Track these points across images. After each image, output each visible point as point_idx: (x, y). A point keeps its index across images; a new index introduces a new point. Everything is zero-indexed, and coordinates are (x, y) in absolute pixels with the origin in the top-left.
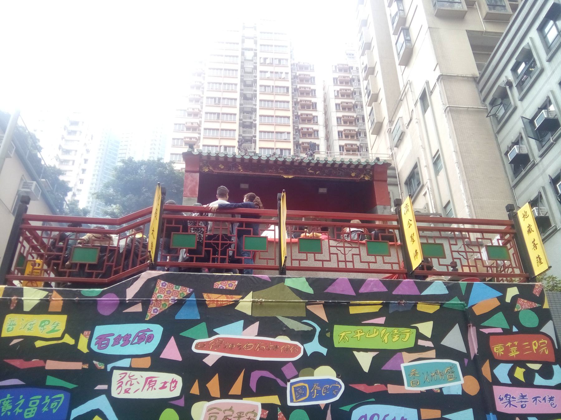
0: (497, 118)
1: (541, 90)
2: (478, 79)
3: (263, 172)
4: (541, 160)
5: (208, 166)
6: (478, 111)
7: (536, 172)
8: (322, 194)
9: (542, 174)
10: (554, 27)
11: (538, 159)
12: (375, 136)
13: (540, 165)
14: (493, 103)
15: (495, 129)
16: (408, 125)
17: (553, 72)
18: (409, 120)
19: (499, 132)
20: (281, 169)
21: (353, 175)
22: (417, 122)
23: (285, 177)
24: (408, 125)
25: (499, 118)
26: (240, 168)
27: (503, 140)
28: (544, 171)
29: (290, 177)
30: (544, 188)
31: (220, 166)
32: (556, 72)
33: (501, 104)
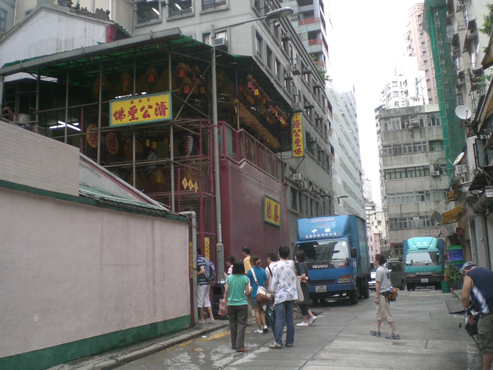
17: (201, 23)
19: (137, 28)
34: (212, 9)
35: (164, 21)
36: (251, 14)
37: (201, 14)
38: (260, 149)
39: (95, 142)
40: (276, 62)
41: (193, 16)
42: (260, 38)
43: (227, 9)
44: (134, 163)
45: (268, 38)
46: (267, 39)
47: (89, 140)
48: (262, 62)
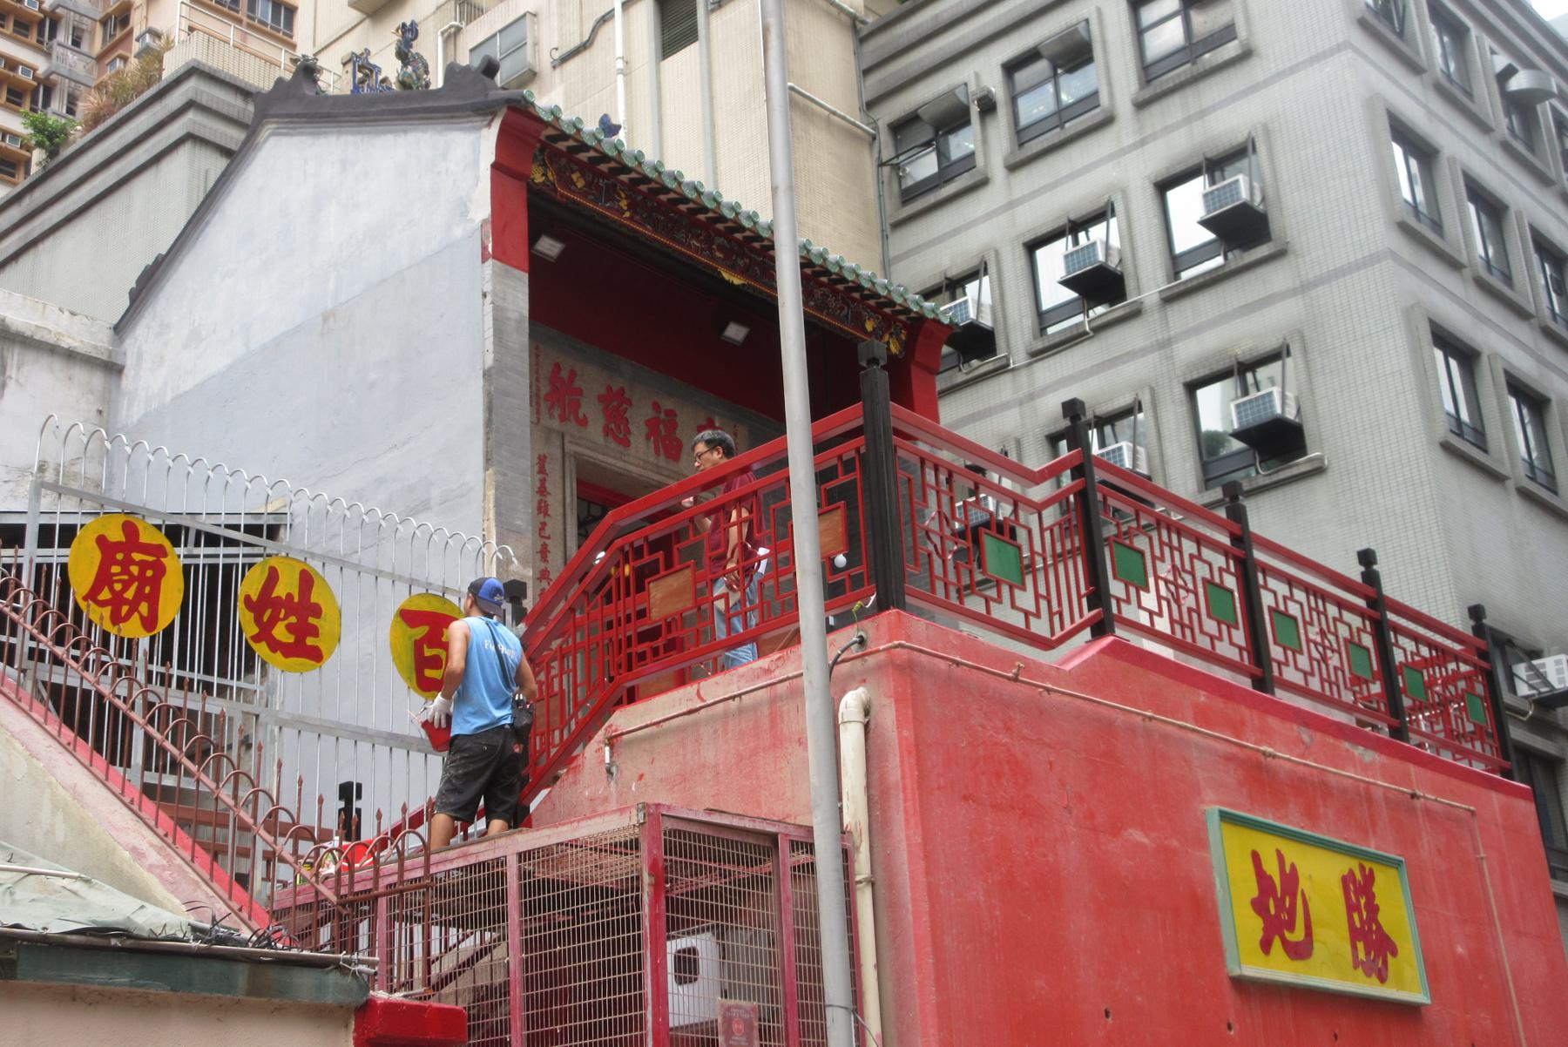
0: (900, 178)
1: (1087, 169)
2: (865, 31)
3: (673, 239)
4: (1029, 365)
5: (545, 165)
6: (850, 134)
7: (1001, 390)
8: (730, 345)
9: (1021, 403)
10: (1178, 21)
11: (1019, 358)
12: (356, 15)
13: (1023, 376)
14: (900, 127)
15: (889, 208)
16: (565, 59)
17: (1143, 142)
18: (575, 42)
19: (898, 225)
20: (721, 248)
21: (869, 326)
22: (621, 72)
23: (726, 276)
24: (565, 59)
25: (909, 182)
26: (624, 204)
27: (907, 255)
28: (1032, 397)
29: (737, 281)
30: (1018, 442)
31: (575, 177)
32: (1150, 147)
33: (928, 144)
34: (1185, 71)
35: (997, 171)
36: (1356, 50)
37: (1141, 105)
38: (1535, 662)
39: (144, 608)
40: (1472, 208)
41: (1108, 121)
42: (1422, 151)
43: (1246, 55)
44: (235, 683)
45: (1489, 160)
46: (1461, 147)
47: (92, 595)
48: (1447, 249)
